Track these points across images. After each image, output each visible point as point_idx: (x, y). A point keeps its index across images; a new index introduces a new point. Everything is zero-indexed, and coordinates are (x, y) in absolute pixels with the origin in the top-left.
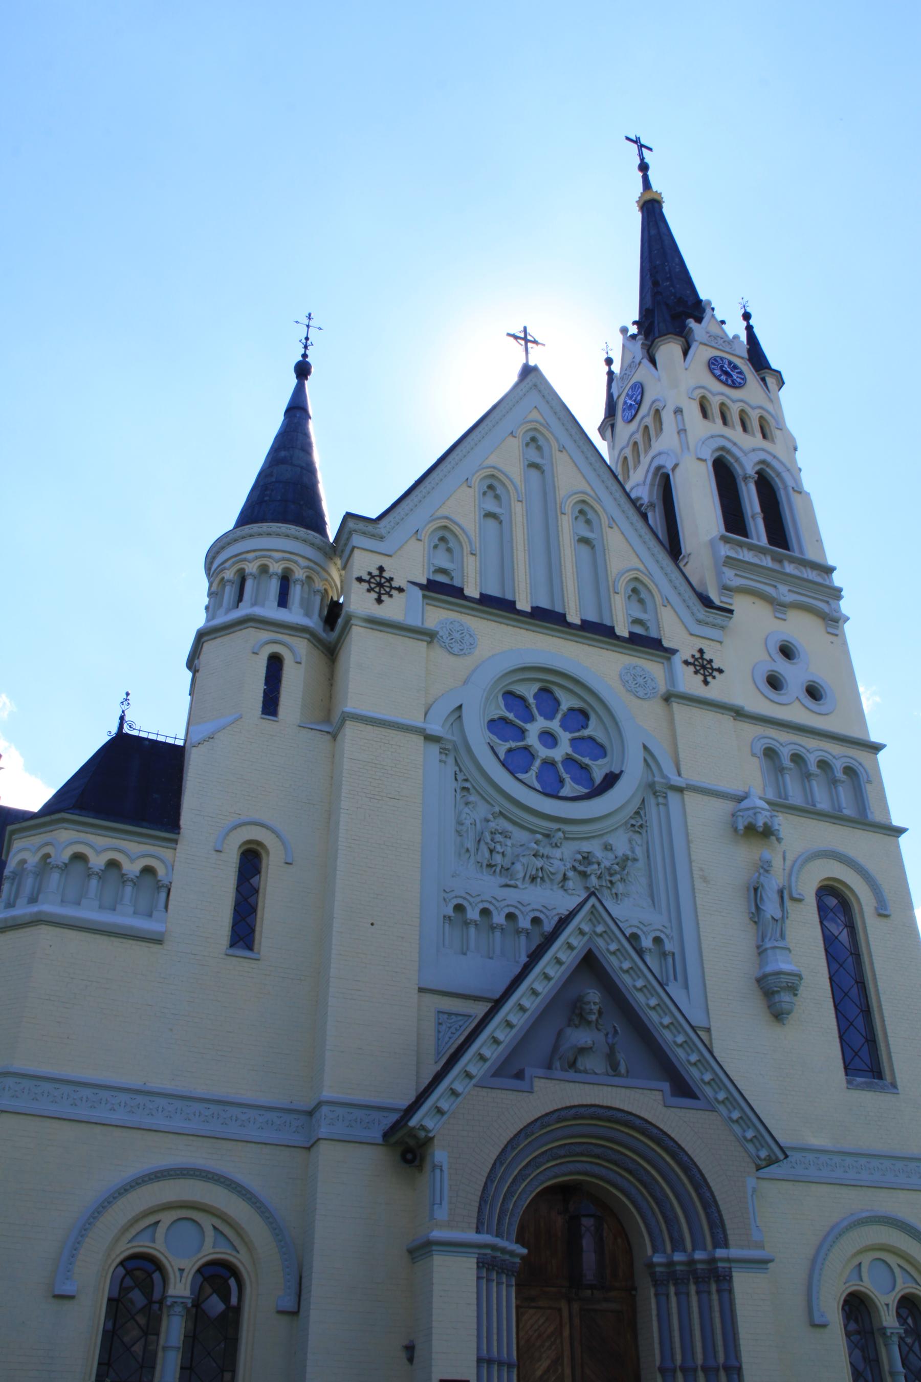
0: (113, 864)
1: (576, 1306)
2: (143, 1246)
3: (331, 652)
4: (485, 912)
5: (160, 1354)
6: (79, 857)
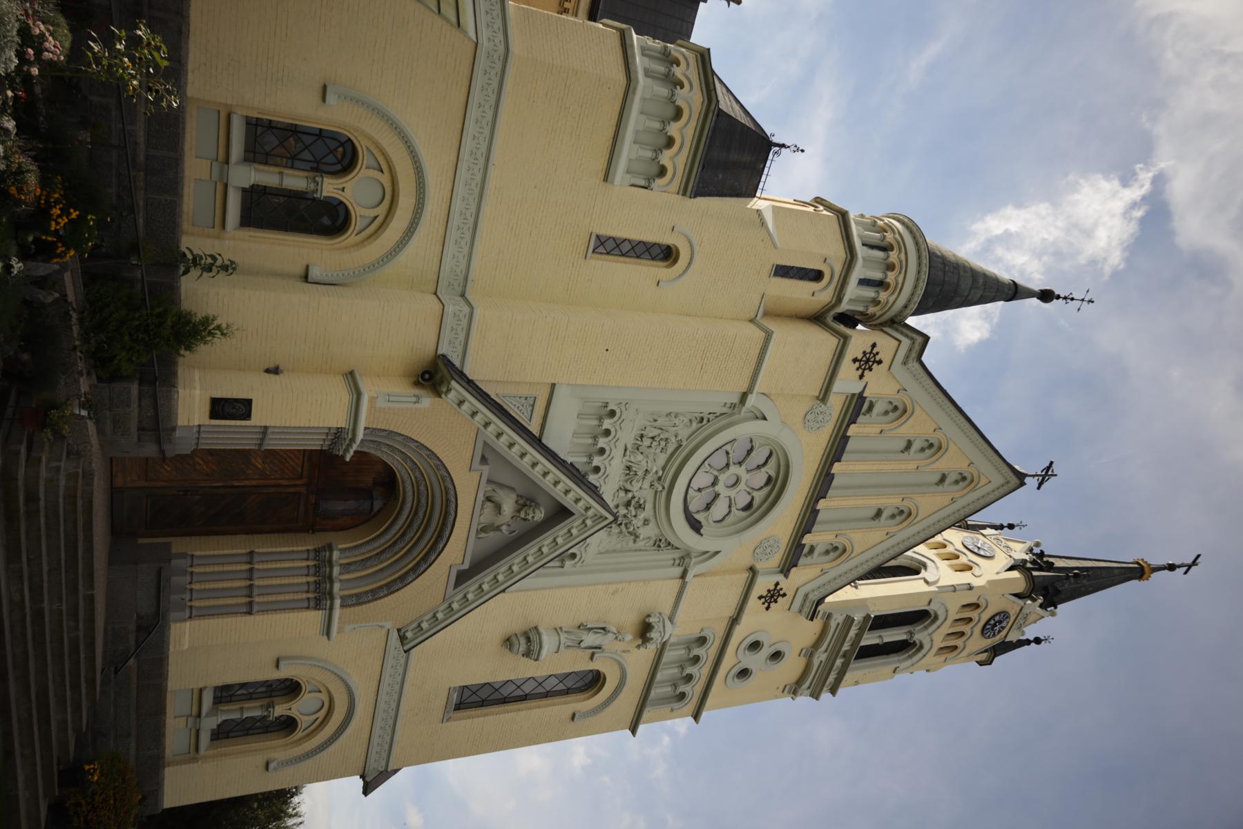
0: (670, 142)
1: (303, 490)
2: (364, 159)
3: (816, 318)
4: (607, 433)
5: (277, 169)
6: (678, 114)
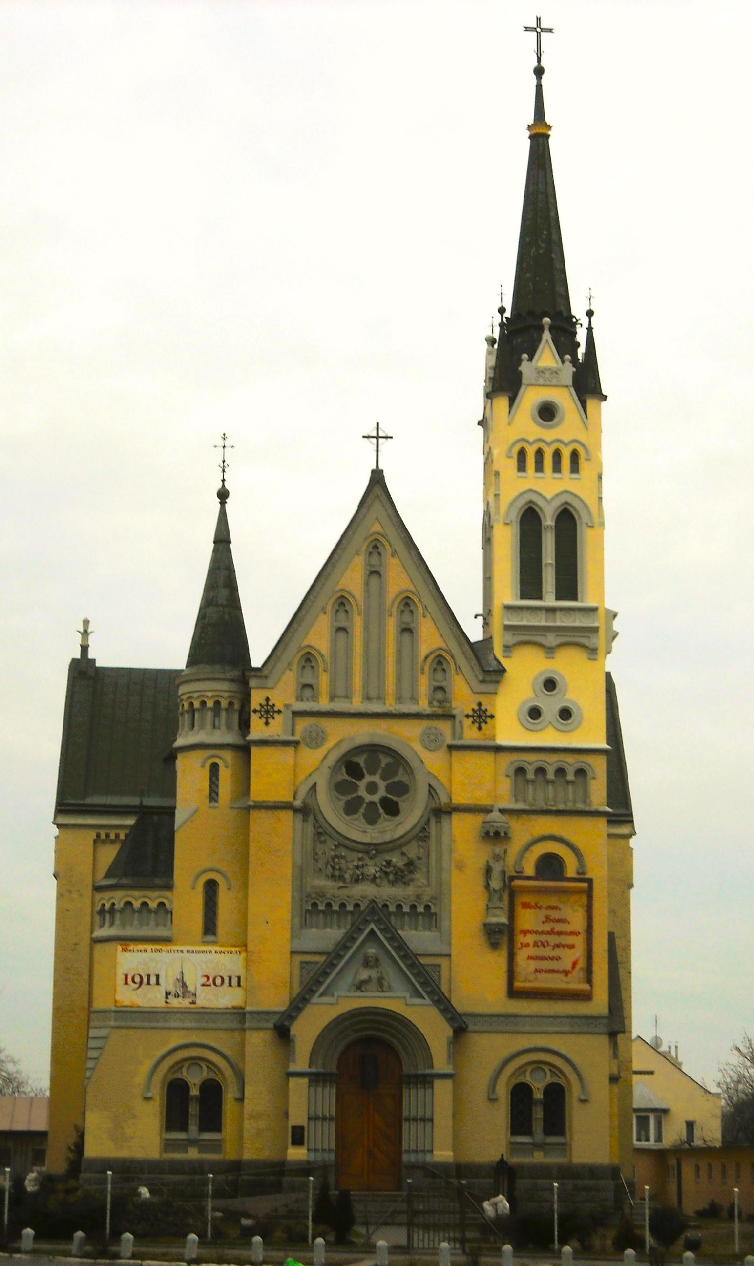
0: (145, 904)
2: (178, 1075)
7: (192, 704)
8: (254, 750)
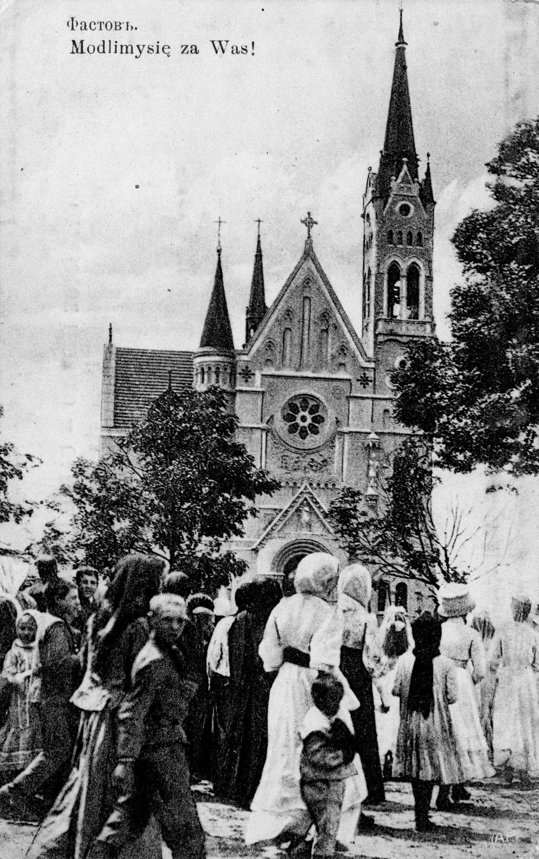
7: (202, 369)
8: (238, 397)
